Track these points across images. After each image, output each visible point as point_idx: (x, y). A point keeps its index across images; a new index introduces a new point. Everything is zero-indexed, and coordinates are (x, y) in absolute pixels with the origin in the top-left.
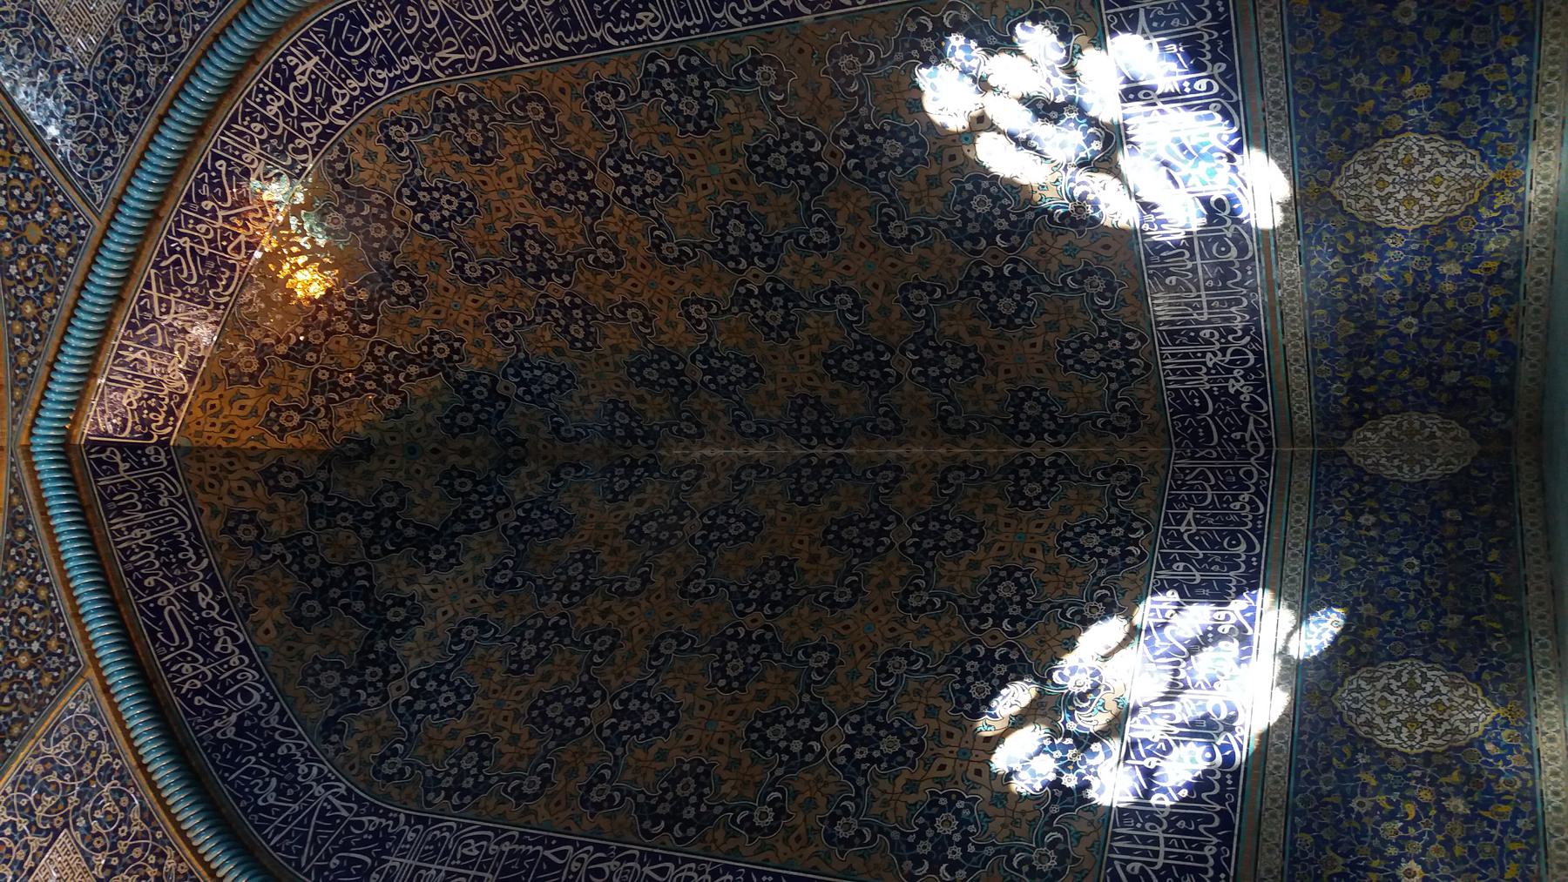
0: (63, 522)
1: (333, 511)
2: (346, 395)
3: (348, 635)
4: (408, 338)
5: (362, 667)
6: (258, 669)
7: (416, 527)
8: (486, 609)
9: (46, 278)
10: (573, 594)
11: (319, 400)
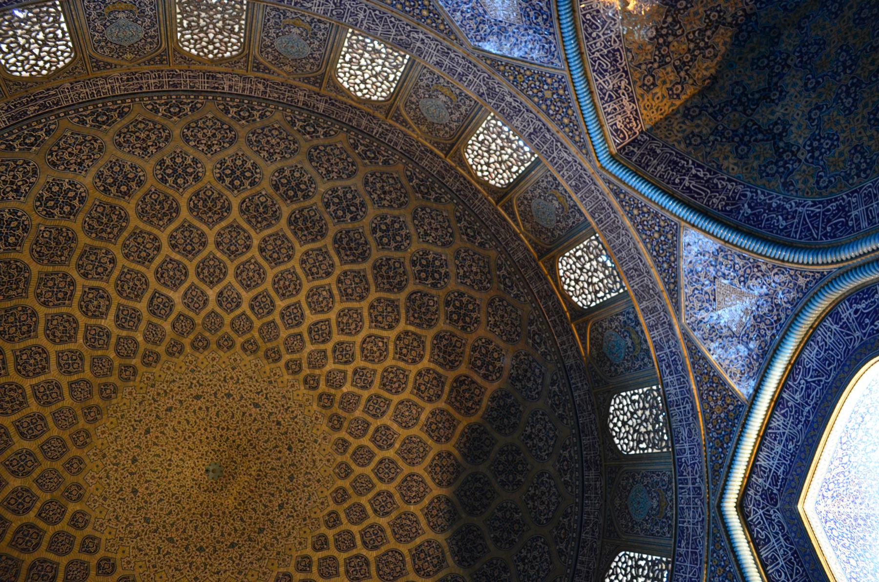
0: (633, 181)
1: (721, 110)
2: (691, 64)
3: (765, 149)
4: (698, 22)
5: (780, 156)
6: (740, 184)
7: (757, 92)
8: (814, 101)
9: (563, 105)
10: (850, 67)
11: (682, 74)
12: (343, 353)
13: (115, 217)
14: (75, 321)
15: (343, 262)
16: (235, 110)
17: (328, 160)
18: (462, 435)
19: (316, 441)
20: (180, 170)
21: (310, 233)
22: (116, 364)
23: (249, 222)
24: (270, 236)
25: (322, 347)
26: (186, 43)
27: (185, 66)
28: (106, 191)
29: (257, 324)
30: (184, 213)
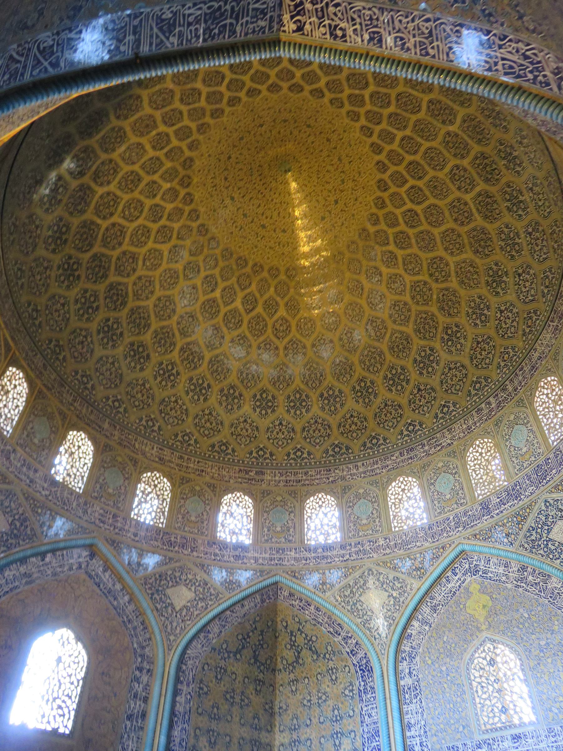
12: (156, 213)
13: (244, 375)
14: (297, 325)
15: (126, 285)
17: (111, 374)
18: (100, 130)
19: (209, 156)
20: (198, 389)
21: (139, 314)
22: (293, 283)
23: (173, 335)
24: (165, 319)
25: (168, 223)
27: (173, 471)
28: (241, 395)
29: (201, 258)
30: (208, 356)
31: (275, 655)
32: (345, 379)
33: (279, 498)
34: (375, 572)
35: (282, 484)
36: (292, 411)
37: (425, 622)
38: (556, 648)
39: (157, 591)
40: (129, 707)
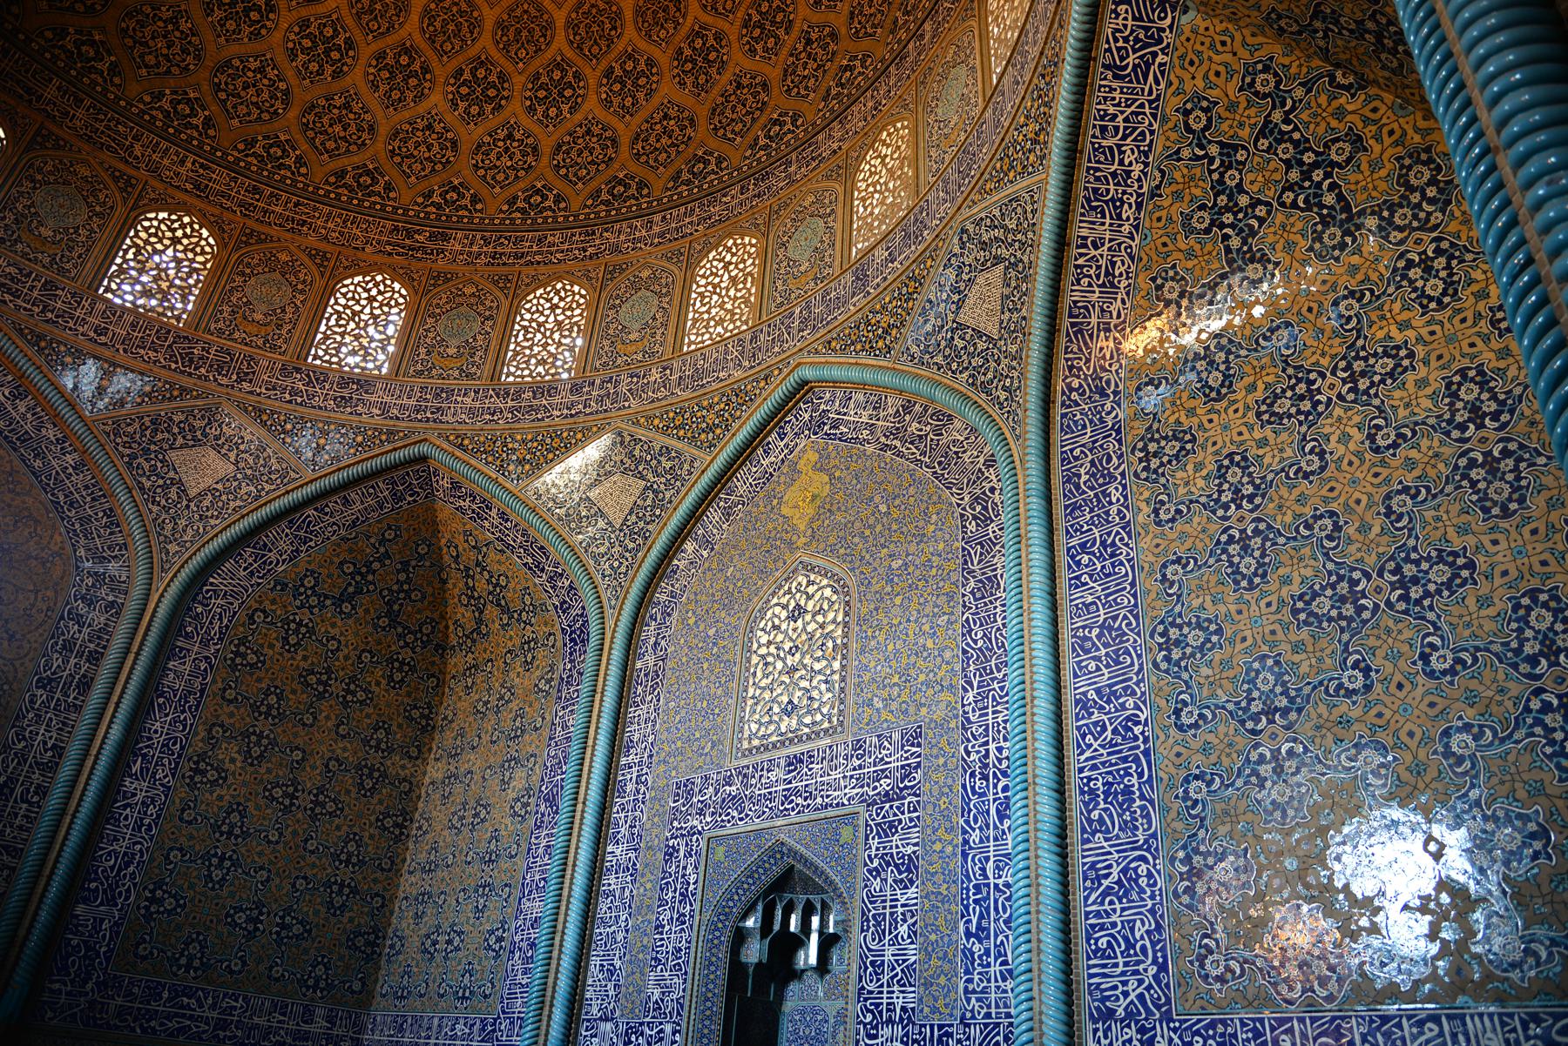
13: (438, 24)
16: (194, 121)
26: (208, 249)
27: (227, 216)
28: (426, 70)
31: (443, 617)
32: (663, 34)
33: (469, 290)
34: (628, 439)
35: (483, 260)
36: (540, 110)
37: (707, 543)
38: (918, 572)
39: (146, 451)
40: (48, 666)
